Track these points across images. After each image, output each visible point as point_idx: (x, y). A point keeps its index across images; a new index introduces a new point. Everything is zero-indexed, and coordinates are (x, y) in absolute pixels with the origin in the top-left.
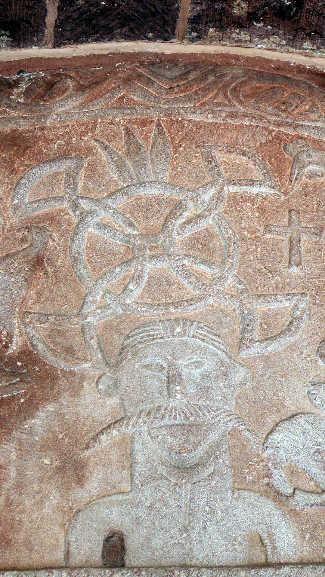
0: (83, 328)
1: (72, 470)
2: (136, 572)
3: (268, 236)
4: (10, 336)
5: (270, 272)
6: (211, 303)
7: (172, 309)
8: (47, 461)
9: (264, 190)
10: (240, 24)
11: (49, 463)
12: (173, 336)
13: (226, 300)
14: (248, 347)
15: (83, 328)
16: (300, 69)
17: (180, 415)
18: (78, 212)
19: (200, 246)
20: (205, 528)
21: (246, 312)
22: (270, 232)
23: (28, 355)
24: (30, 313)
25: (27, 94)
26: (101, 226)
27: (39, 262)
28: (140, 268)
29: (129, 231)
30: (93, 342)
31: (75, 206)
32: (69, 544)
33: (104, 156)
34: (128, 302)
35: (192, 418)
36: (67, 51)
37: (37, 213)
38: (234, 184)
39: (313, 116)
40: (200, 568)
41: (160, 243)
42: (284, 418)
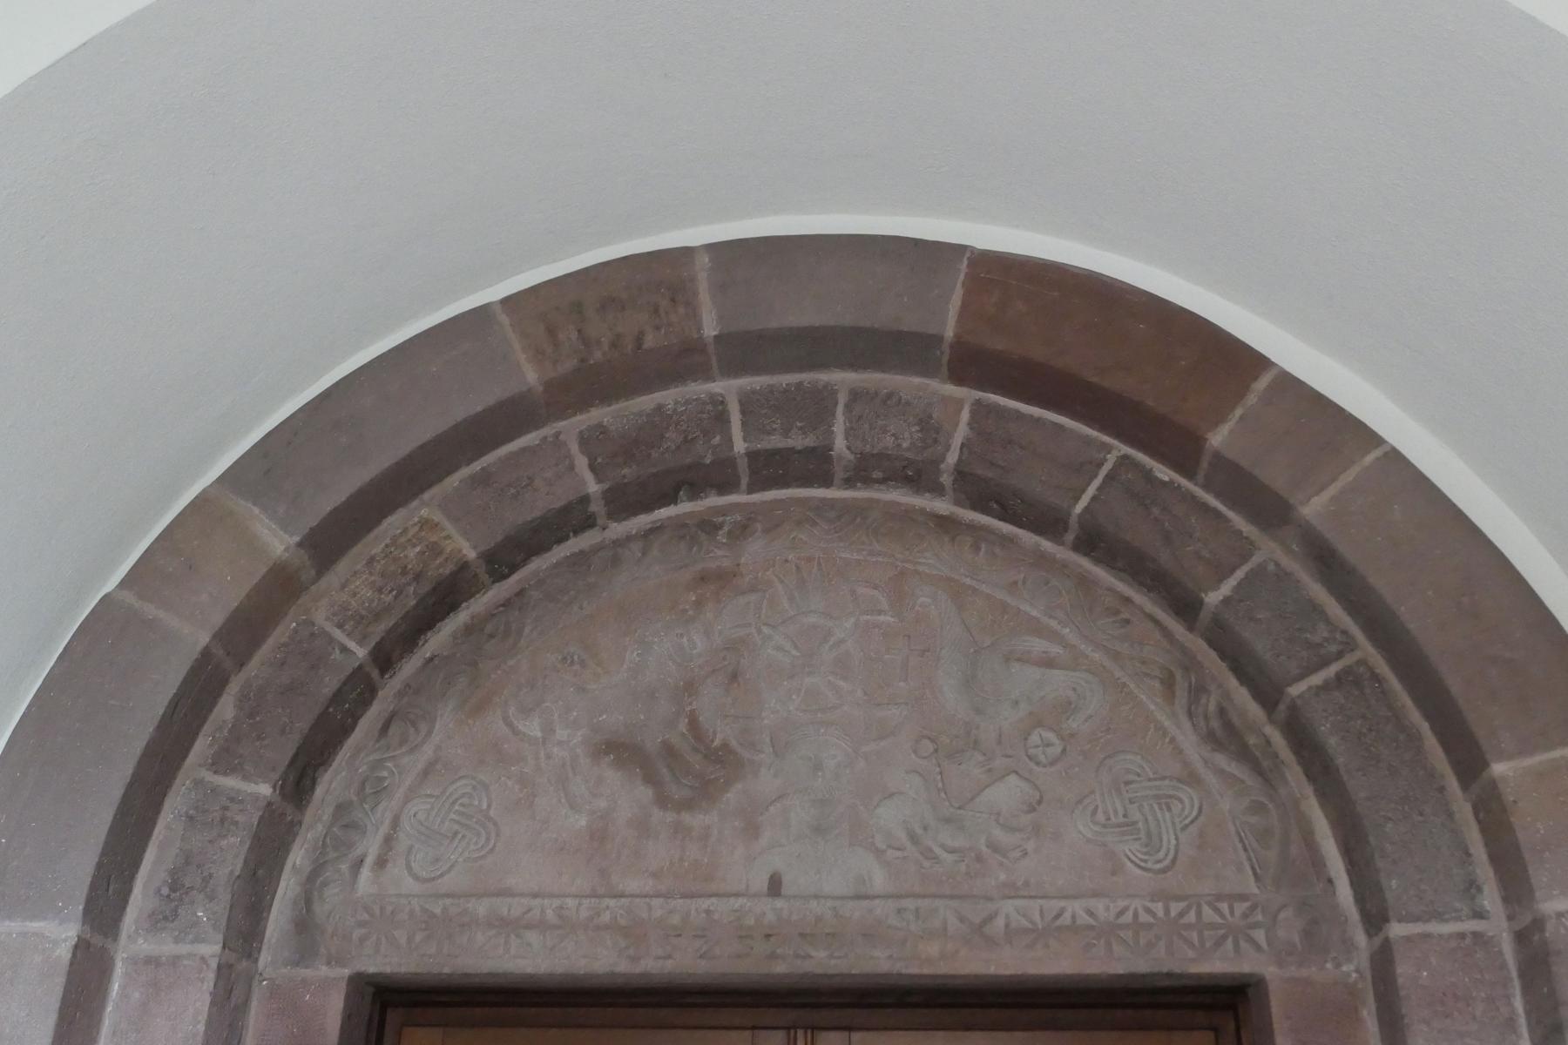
1: (752, 830)
4: (715, 733)
10: (878, 481)
16: (922, 511)
23: (725, 746)
25: (730, 532)
26: (779, 648)
27: (734, 677)
31: (759, 631)
33: (780, 587)
36: (756, 497)
39: (928, 554)
40: (826, 897)
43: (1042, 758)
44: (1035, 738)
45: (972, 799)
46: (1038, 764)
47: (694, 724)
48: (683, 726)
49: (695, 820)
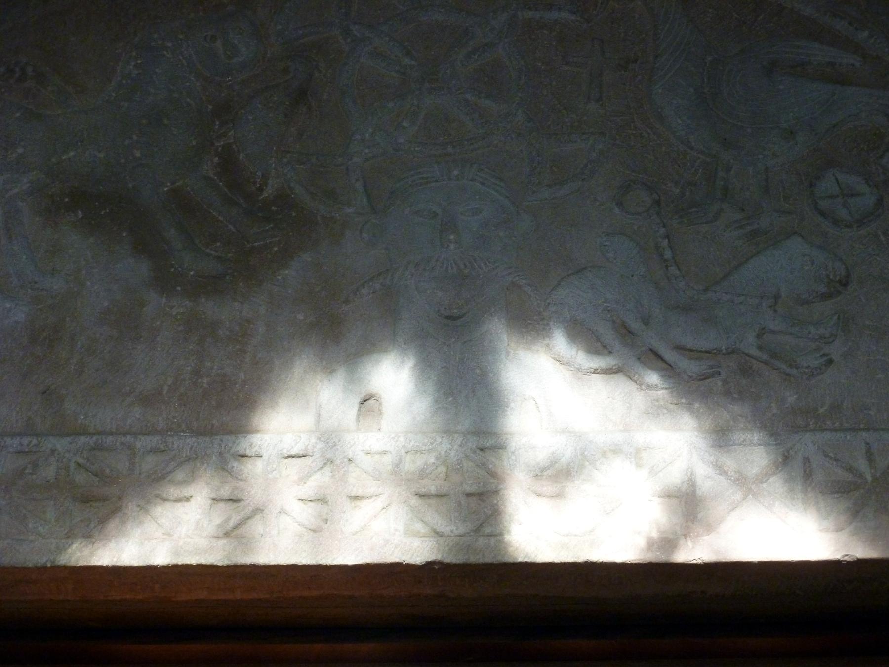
0: (347, 170)
2: (393, 438)
3: (567, 68)
4: (265, 177)
5: (565, 109)
6: (496, 142)
7: (450, 149)
8: (300, 317)
9: (564, 15)
11: (302, 318)
12: (450, 179)
13: (512, 139)
14: (534, 192)
15: (347, 170)
17: (452, 268)
18: (349, 40)
19: (486, 79)
20: (473, 392)
21: (534, 153)
22: (567, 64)
24: (289, 152)
28: (415, 102)
29: (407, 61)
30: (359, 185)
32: (320, 406)
34: (402, 141)
35: (466, 271)
37: (301, 41)
38: (530, 9)
41: (440, 75)
42: (570, 272)
43: (843, 213)
44: (827, 185)
45: (726, 276)
46: (836, 223)
47: (228, 164)
48: (209, 167)
49: (223, 312)
